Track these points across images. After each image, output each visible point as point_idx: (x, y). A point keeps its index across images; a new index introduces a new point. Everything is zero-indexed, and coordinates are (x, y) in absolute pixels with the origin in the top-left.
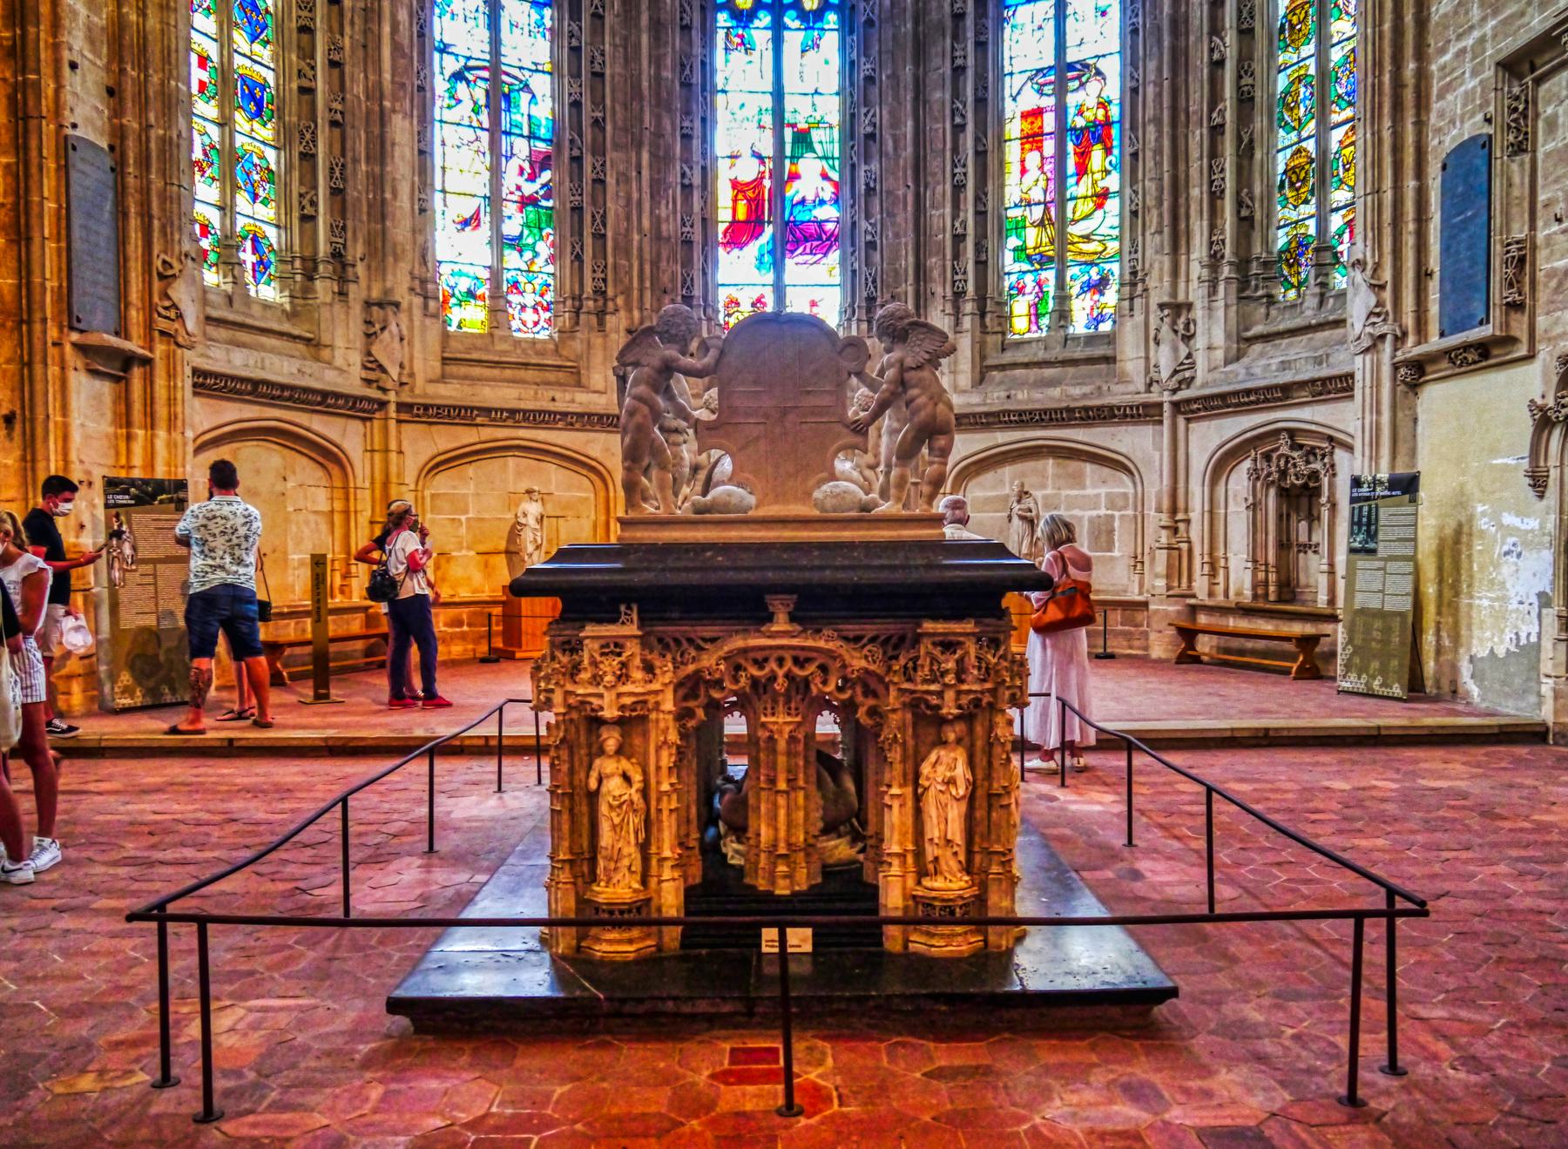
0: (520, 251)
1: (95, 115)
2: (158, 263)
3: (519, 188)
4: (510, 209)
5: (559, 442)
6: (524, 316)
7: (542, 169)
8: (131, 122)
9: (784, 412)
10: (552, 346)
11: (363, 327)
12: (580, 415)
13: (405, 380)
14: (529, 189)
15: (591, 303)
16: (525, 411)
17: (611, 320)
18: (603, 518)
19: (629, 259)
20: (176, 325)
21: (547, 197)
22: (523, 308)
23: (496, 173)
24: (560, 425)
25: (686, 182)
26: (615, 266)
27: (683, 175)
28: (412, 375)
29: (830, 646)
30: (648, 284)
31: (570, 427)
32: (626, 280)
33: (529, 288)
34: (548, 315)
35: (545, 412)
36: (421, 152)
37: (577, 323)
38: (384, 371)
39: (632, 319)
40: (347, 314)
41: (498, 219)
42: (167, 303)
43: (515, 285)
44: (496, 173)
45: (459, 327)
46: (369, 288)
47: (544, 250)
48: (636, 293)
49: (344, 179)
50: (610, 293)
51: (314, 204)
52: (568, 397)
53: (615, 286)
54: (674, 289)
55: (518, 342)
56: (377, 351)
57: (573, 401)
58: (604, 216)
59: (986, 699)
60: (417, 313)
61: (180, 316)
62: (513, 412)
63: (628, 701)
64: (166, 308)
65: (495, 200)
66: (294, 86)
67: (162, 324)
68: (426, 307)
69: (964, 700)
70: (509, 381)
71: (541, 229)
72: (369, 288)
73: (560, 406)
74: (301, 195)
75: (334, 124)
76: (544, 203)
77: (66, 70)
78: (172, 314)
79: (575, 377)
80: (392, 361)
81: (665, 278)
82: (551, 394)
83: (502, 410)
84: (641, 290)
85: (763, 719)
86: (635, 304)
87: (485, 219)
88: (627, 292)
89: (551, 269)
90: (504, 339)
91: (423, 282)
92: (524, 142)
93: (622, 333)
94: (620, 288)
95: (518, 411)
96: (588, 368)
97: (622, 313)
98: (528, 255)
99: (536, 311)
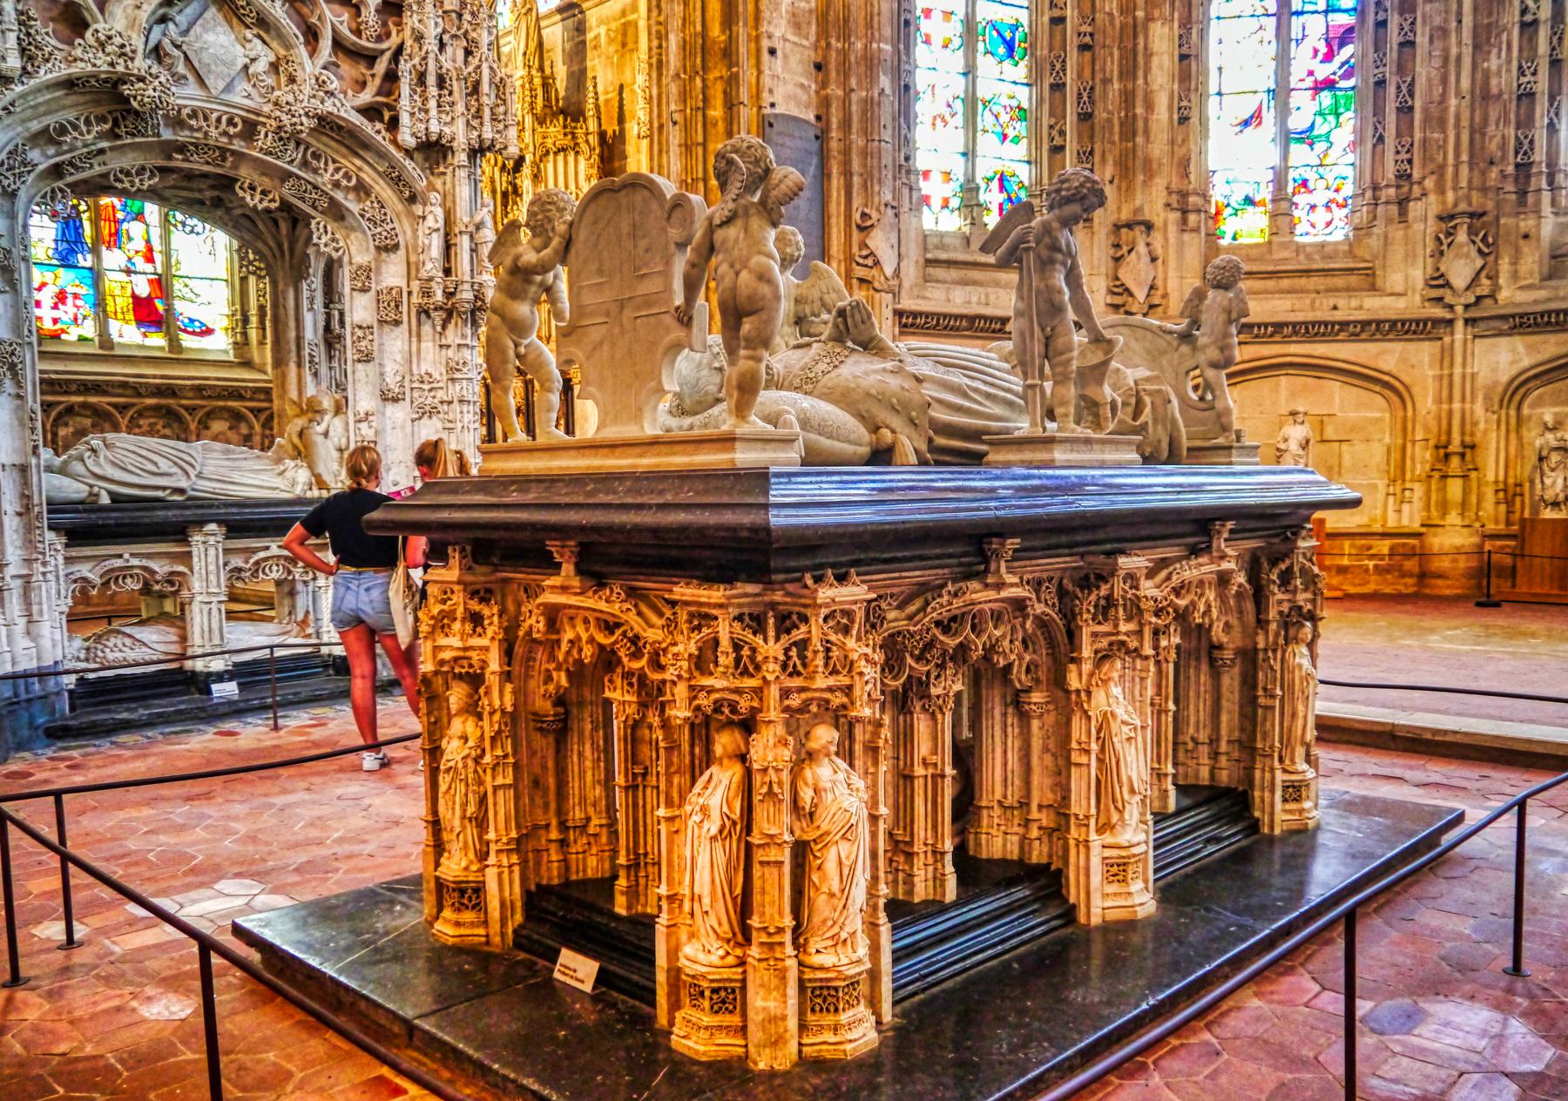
0: (1311, 144)
1: (799, 91)
2: (857, 217)
3: (1311, 73)
4: (1296, 99)
5: (1341, 356)
6: (1312, 217)
7: (1342, 45)
8: (835, 91)
9: (621, 305)
10: (1346, 248)
11: (1112, 252)
12: (1365, 324)
13: (1156, 302)
14: (1324, 71)
15: (1392, 191)
16: (1294, 324)
17: (1415, 209)
18: (1400, 441)
19: (1444, 131)
20: (874, 272)
21: (1347, 75)
22: (1313, 207)
23: (1283, 60)
24: (1342, 336)
25: (1529, 18)
26: (1424, 140)
27: (1524, 11)
28: (1165, 296)
29: (615, 608)
30: (1464, 157)
31: (1355, 337)
32: (1440, 159)
33: (1321, 184)
34: (1346, 211)
35: (1320, 323)
36: (1183, 57)
37: (1375, 218)
38: (1131, 295)
39: (1444, 203)
40: (1092, 239)
41: (1284, 111)
42: (864, 253)
43: (1304, 183)
44: (1283, 60)
45: (1234, 238)
46: (1119, 209)
47: (1344, 134)
48: (1450, 170)
49: (1092, 103)
50: (1416, 175)
51: (1062, 133)
52: (1354, 303)
53: (1424, 166)
54: (1504, 157)
55: (1299, 248)
56: (1126, 276)
57: (1361, 308)
58: (1412, 84)
59: (744, 704)
60: (1172, 230)
61: (877, 263)
62: (1279, 326)
63: (447, 655)
64: (866, 257)
65: (1281, 93)
66: (1046, 19)
67: (860, 272)
68: (1184, 221)
69: (704, 701)
70: (1281, 292)
71: (1338, 115)
72: (1119, 209)
73: (1339, 316)
74: (1051, 127)
75: (1084, 48)
76: (1343, 84)
77: (765, 56)
78: (870, 262)
79: (1369, 279)
80: (1140, 285)
81: (1493, 146)
82: (1332, 302)
83: (1266, 325)
84: (1457, 166)
85: (608, 694)
86: (1449, 184)
87: (1269, 117)
88: (1440, 171)
89: (1351, 158)
90: (1284, 246)
91: (1184, 195)
92: (1321, 17)
93: (1431, 221)
94: (1431, 166)
95: (1287, 324)
96: (1384, 267)
97: (1432, 198)
98: (1320, 147)
99: (1327, 207)
